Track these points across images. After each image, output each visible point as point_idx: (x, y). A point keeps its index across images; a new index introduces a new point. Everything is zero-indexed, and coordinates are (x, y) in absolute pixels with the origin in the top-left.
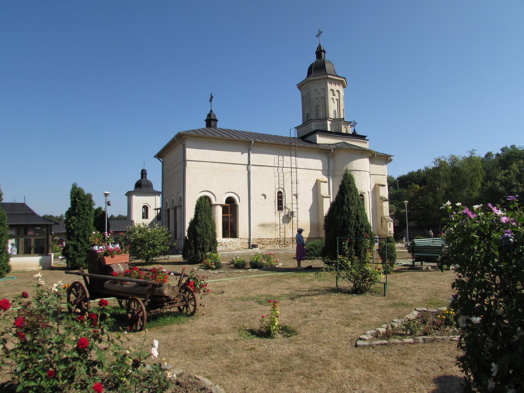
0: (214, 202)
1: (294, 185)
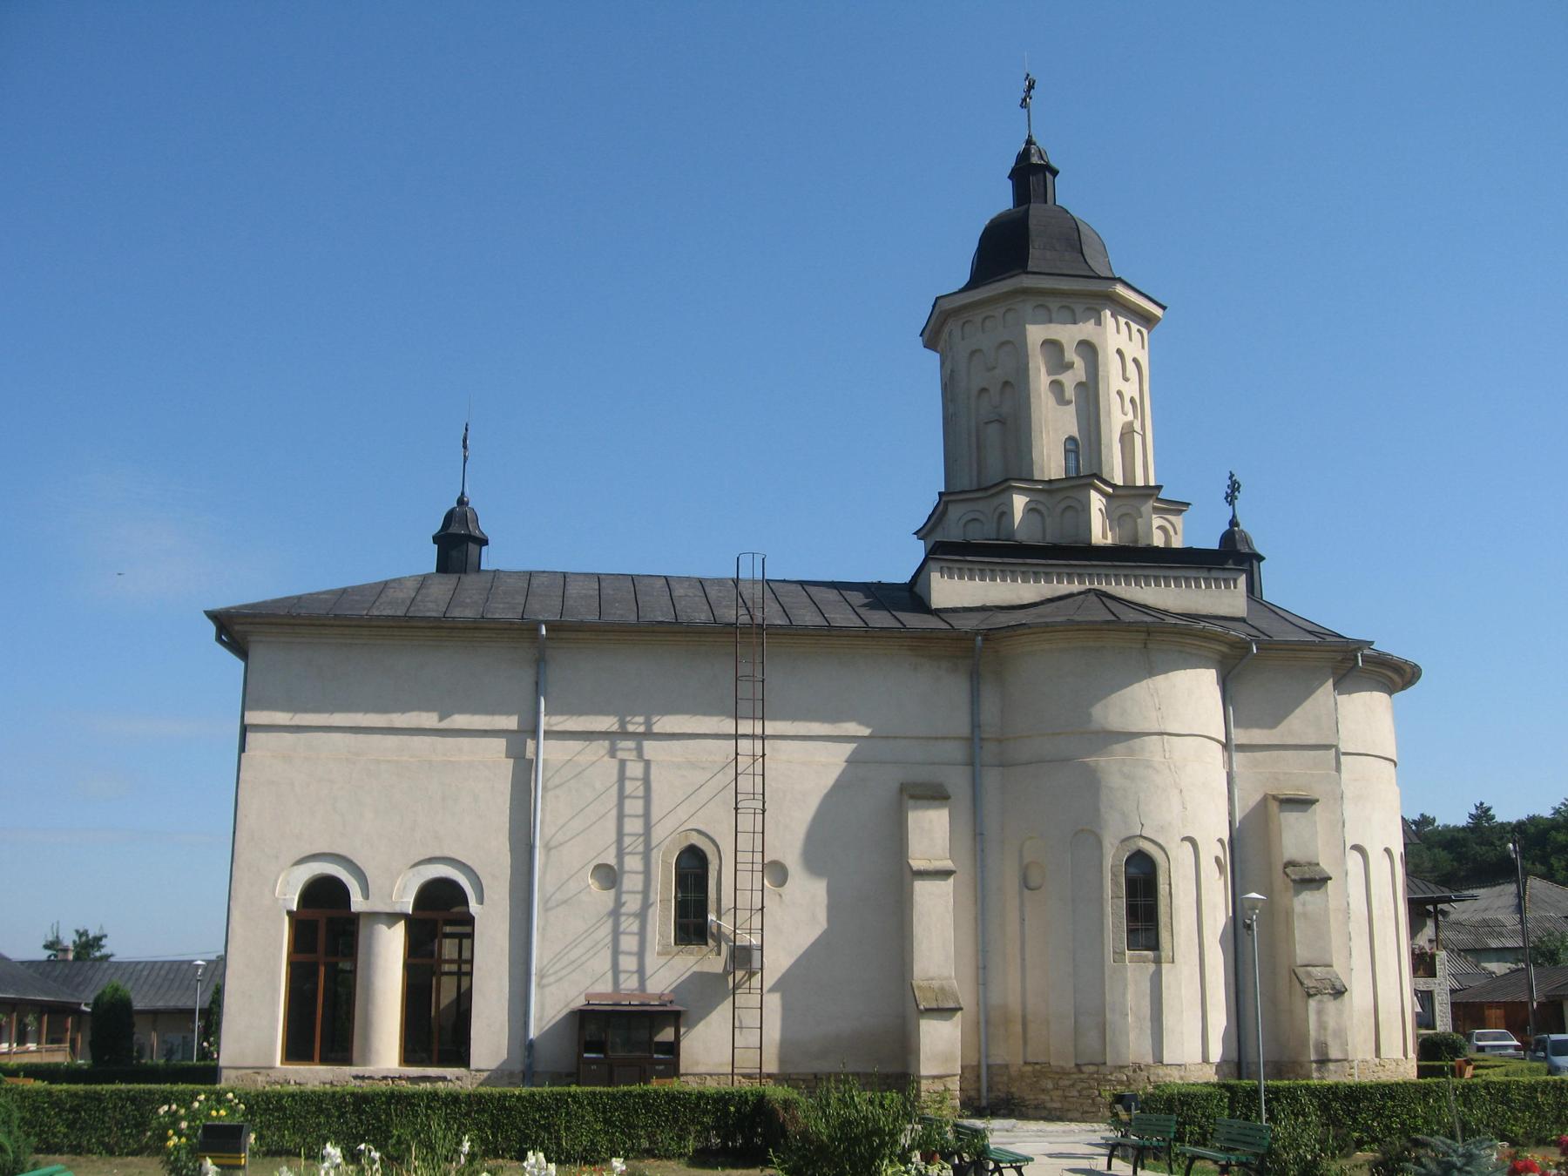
0: (358, 903)
1: (746, 822)
